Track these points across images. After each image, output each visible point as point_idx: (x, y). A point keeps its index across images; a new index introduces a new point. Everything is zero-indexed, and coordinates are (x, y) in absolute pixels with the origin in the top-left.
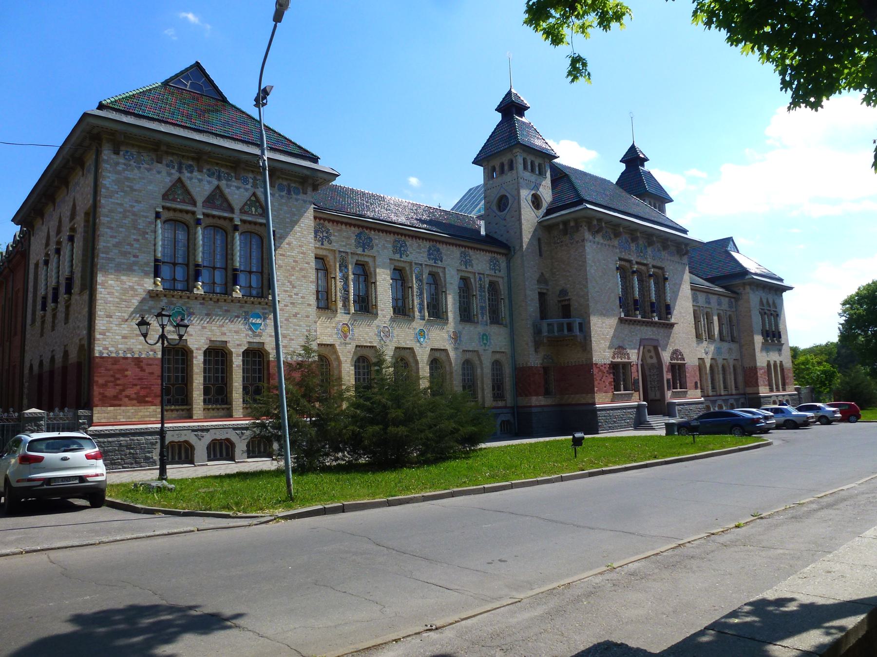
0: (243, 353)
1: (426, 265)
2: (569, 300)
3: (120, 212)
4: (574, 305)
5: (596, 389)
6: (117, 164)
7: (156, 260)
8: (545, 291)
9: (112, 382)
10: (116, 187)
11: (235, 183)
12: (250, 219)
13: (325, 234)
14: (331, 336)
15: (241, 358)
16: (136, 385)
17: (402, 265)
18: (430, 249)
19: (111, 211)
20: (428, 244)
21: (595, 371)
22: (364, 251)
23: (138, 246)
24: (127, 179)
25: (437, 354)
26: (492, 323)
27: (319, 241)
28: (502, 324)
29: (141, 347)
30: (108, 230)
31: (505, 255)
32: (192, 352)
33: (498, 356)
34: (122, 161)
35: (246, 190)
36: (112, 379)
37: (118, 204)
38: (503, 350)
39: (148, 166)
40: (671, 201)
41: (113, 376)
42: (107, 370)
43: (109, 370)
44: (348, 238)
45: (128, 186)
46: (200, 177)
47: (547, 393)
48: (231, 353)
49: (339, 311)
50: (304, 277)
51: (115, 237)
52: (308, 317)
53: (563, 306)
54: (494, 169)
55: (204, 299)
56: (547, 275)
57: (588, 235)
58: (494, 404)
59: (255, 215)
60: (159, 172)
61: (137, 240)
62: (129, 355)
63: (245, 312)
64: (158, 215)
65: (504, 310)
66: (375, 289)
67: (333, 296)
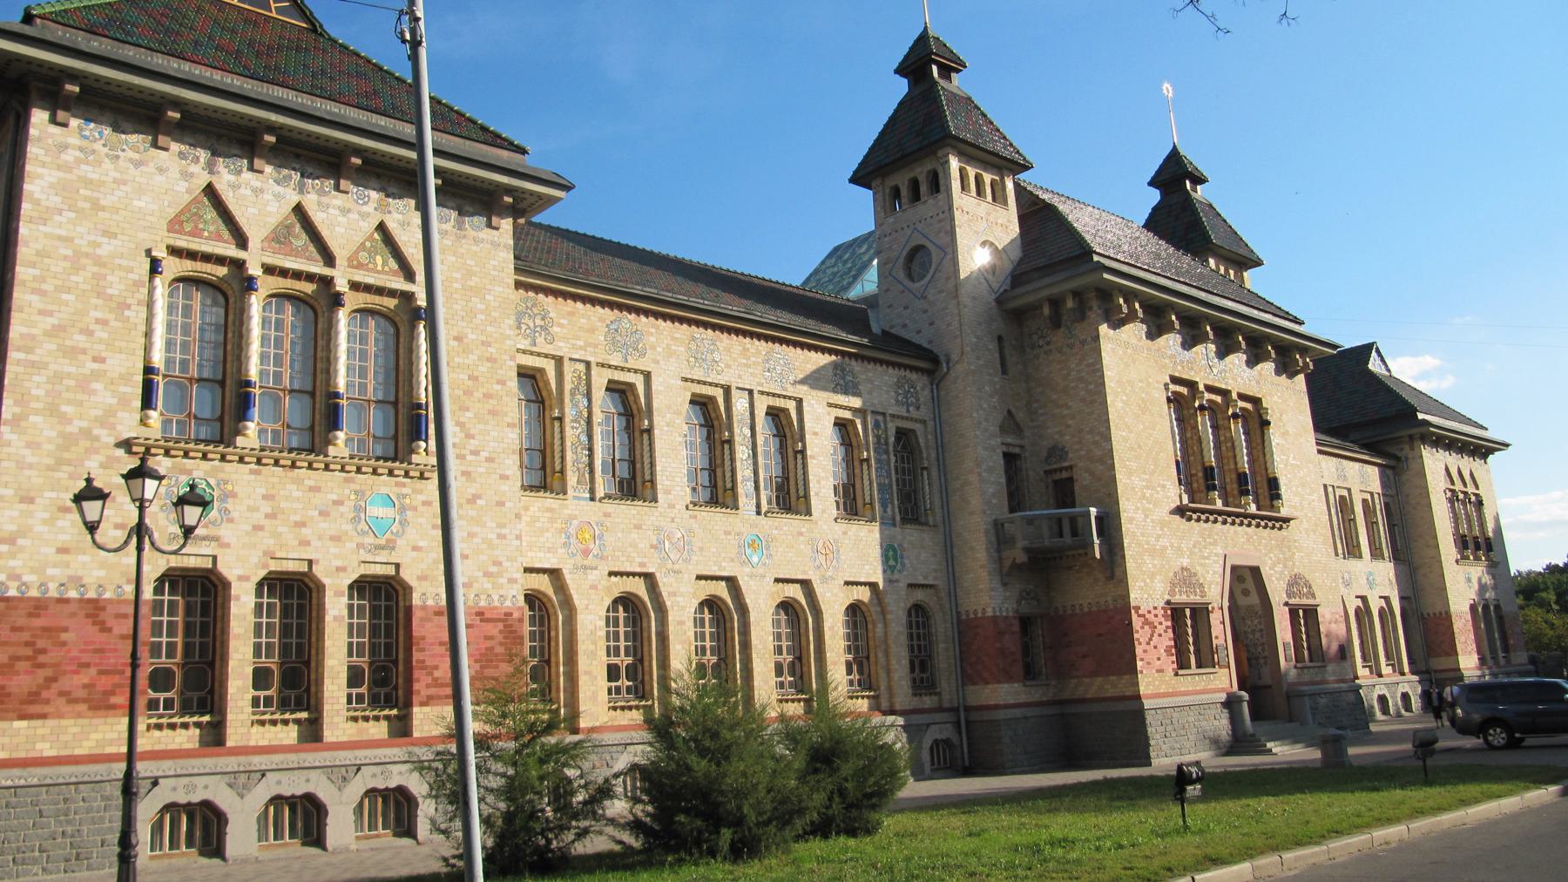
0: (351, 587)
1: (762, 393)
2: (1071, 467)
3: (66, 258)
4: (1083, 480)
5: (1139, 664)
6: (64, 147)
7: (149, 370)
8: (1017, 450)
9: (27, 658)
10: (58, 199)
11: (338, 200)
12: (370, 280)
13: (539, 322)
15: (345, 600)
16: (88, 665)
17: (709, 391)
19: (38, 254)
21: (1136, 622)
23: (105, 335)
24: (88, 182)
26: (905, 521)
27: (526, 337)
28: (926, 524)
29: (102, 573)
30: (35, 298)
31: (930, 373)
32: (226, 585)
33: (919, 595)
34: (74, 140)
35: (364, 216)
36: (29, 652)
37: (60, 238)
39: (136, 156)
40: (1258, 263)
41: (27, 644)
42: (14, 629)
43: (21, 629)
44: (592, 330)
45: (86, 199)
46: (258, 184)
47: (1030, 673)
48: (321, 588)
49: (570, 492)
50: (493, 413)
51: (50, 314)
52: (501, 504)
53: (1055, 482)
54: (896, 193)
55: (259, 462)
56: (1020, 416)
57: (1104, 329)
58: (915, 703)
59: (383, 272)
60: (161, 170)
61: (103, 323)
62: (73, 594)
63: (356, 493)
64: (155, 267)
65: (930, 494)
66: (651, 445)
67: (558, 461)
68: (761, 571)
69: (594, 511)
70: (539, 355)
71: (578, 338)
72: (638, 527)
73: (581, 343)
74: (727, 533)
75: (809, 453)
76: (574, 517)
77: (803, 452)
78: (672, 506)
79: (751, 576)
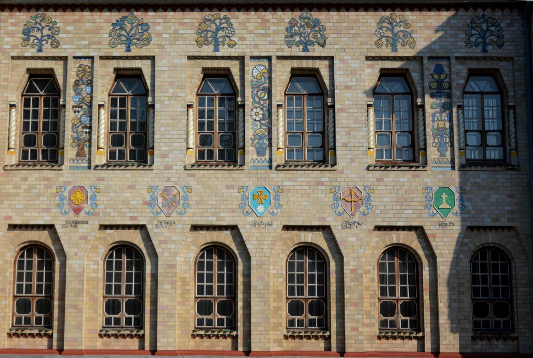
13: (46, 32)
14: (47, 210)
17: (223, 64)
18: (293, 23)
20: (287, 16)
22: (128, 49)
25: (309, 237)
27: (33, 46)
38: (504, 222)
44: (97, 31)
49: (67, 164)
68: (266, 219)
69: (87, 179)
70: (47, 58)
71: (83, 39)
72: (132, 187)
73: (86, 43)
74: (228, 187)
75: (337, 107)
76: (68, 183)
77: (333, 107)
78: (168, 168)
79: (254, 224)
